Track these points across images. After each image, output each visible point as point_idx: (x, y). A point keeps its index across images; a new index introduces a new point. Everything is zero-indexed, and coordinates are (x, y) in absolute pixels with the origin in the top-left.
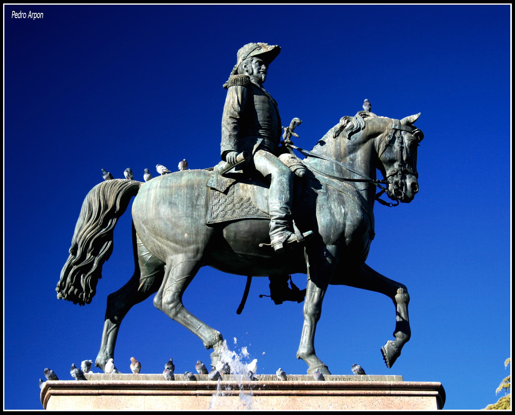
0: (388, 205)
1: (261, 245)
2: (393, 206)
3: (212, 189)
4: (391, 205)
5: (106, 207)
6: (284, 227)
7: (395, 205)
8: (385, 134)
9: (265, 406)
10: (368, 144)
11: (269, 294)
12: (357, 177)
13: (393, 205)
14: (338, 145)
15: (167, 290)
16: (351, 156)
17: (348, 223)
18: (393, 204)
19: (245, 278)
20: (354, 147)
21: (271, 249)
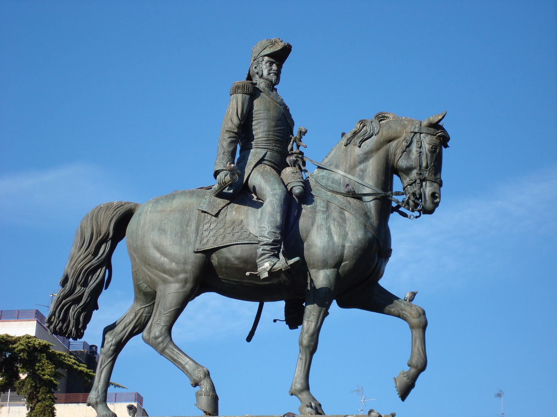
1: (248, 274)
3: (203, 212)
4: (412, 217)
5: (99, 234)
6: (271, 253)
7: (417, 217)
8: (402, 139)
10: (382, 152)
11: (284, 319)
12: (367, 191)
15: (156, 323)
16: (362, 166)
17: (347, 245)
19: (257, 304)
20: (365, 156)
21: (257, 277)
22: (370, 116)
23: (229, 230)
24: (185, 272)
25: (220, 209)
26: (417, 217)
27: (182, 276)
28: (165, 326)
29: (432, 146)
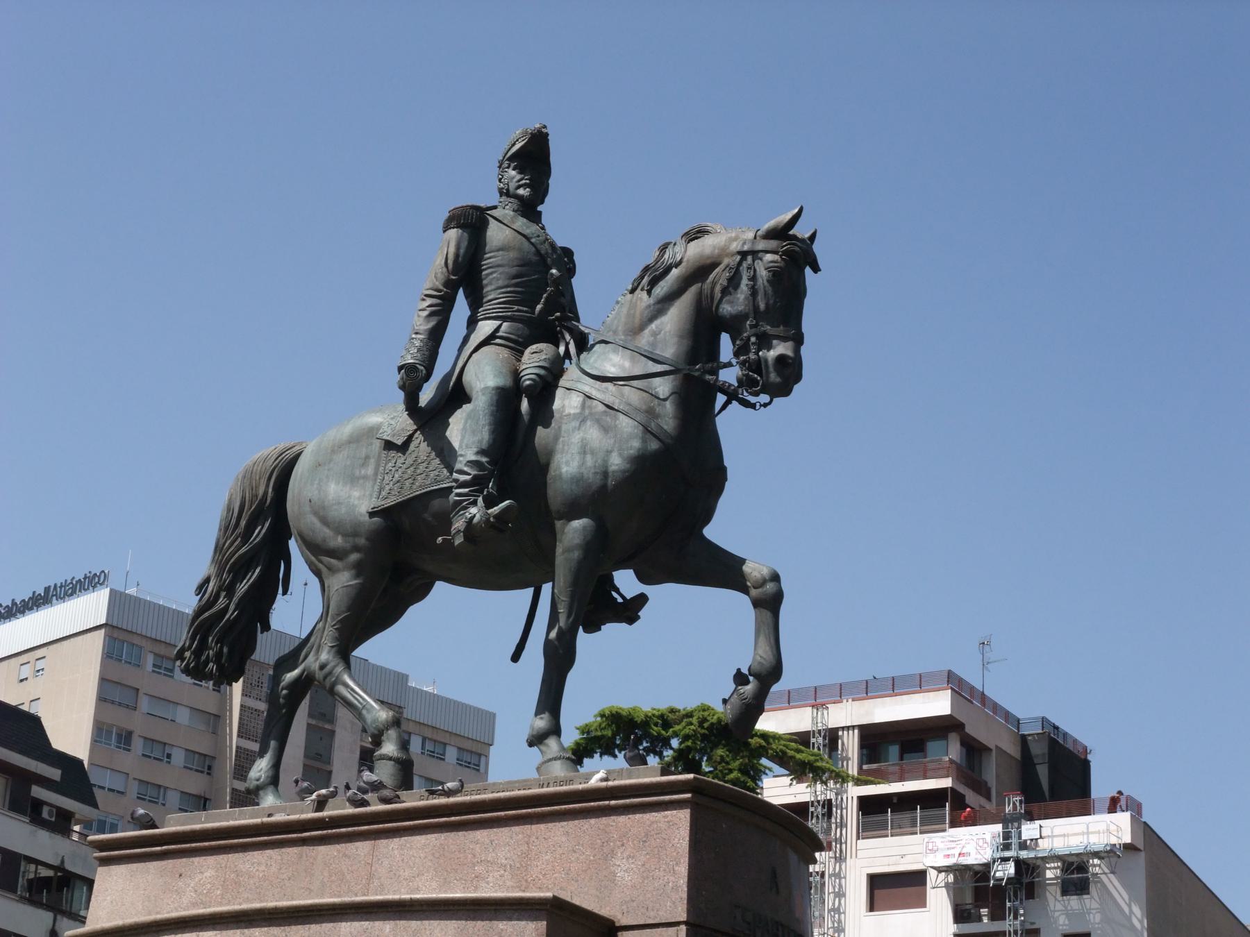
0: (753, 406)
2: (762, 407)
4: (758, 407)
7: (765, 405)
9: (406, 851)
13: (761, 405)
14: (633, 306)
16: (653, 326)
18: (762, 403)
20: (659, 306)
22: (675, 235)
23: (422, 468)
24: (356, 549)
26: (765, 405)
27: (354, 557)
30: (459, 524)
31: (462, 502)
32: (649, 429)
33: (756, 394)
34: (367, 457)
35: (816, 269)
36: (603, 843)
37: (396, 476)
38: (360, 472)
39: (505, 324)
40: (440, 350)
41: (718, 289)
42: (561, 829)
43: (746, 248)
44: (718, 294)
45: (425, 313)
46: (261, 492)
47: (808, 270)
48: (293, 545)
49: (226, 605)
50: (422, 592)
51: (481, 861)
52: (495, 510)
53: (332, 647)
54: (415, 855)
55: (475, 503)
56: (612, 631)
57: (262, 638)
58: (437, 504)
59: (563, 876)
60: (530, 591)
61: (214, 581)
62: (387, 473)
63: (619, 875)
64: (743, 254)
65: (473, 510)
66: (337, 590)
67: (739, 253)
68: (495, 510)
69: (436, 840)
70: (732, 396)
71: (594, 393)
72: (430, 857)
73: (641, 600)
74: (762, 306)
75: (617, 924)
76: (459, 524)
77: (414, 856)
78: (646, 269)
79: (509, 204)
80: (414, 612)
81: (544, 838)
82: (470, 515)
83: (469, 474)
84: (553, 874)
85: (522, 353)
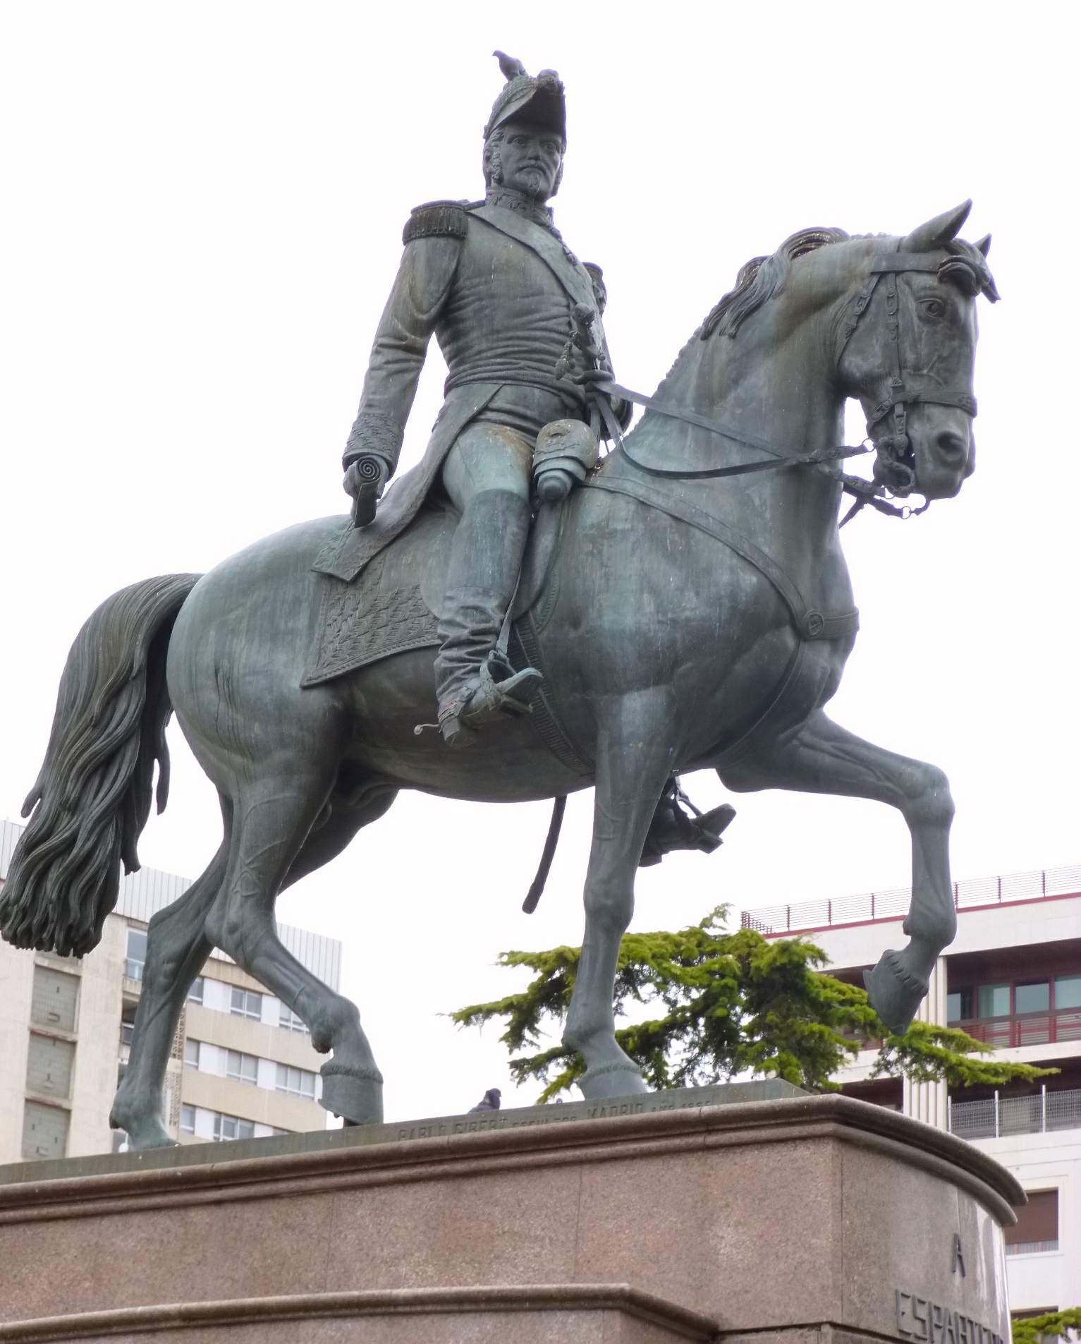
0: (898, 513)
1: (418, 729)
2: (913, 514)
4: (906, 513)
6: (464, 667)
7: (918, 511)
9: (383, 1218)
13: (911, 512)
23: (384, 616)
24: (283, 743)
25: (366, 561)
26: (918, 511)
27: (280, 756)
28: (252, 896)
29: (929, 303)
30: (450, 704)
31: (451, 671)
32: (742, 553)
33: (904, 495)
34: (297, 601)
35: (992, 296)
36: (697, 1202)
37: (344, 627)
38: (286, 623)
39: (507, 389)
40: (407, 431)
41: (841, 331)
42: (628, 1181)
43: (883, 266)
44: (842, 340)
45: (383, 373)
46: (123, 654)
47: (981, 299)
48: (174, 734)
49: (72, 834)
50: (377, 806)
51: (504, 1233)
52: (508, 683)
53: (247, 897)
54: (398, 1224)
55: (476, 671)
56: (678, 861)
57: (127, 883)
58: (407, 668)
59: (634, 1254)
60: (551, 802)
61: (52, 794)
62: (330, 625)
63: (722, 1251)
64: (882, 275)
65: (473, 683)
66: (254, 808)
67: (873, 274)
68: (508, 683)
69: (431, 1200)
70: (864, 494)
71: (655, 499)
72: (422, 1228)
73: (722, 816)
74: (910, 357)
75: (726, 1327)
76: (450, 704)
77: (396, 1226)
78: (727, 301)
79: (504, 198)
80: (367, 837)
81: (603, 1196)
82: (469, 692)
83: (464, 627)
84: (619, 1251)
85: (535, 434)
